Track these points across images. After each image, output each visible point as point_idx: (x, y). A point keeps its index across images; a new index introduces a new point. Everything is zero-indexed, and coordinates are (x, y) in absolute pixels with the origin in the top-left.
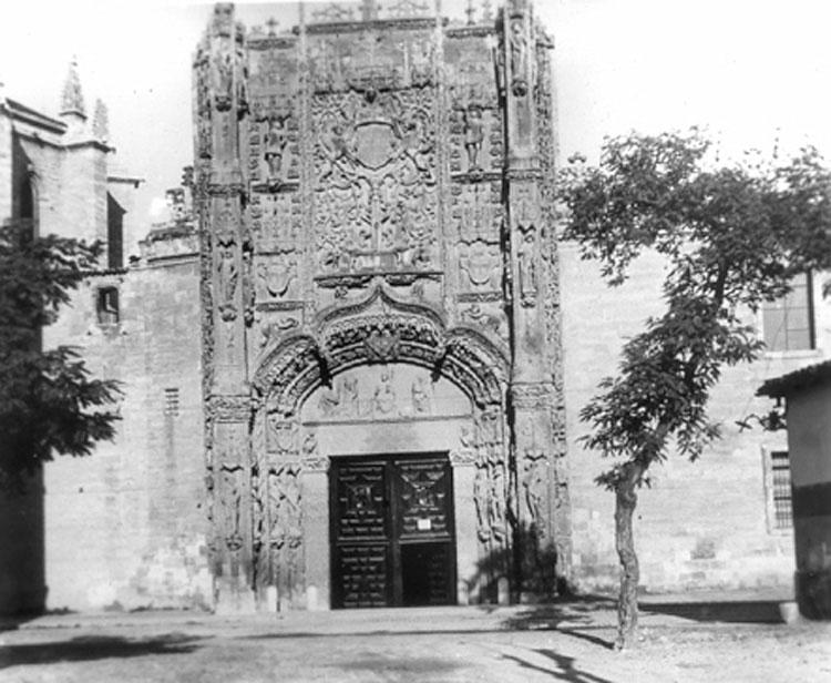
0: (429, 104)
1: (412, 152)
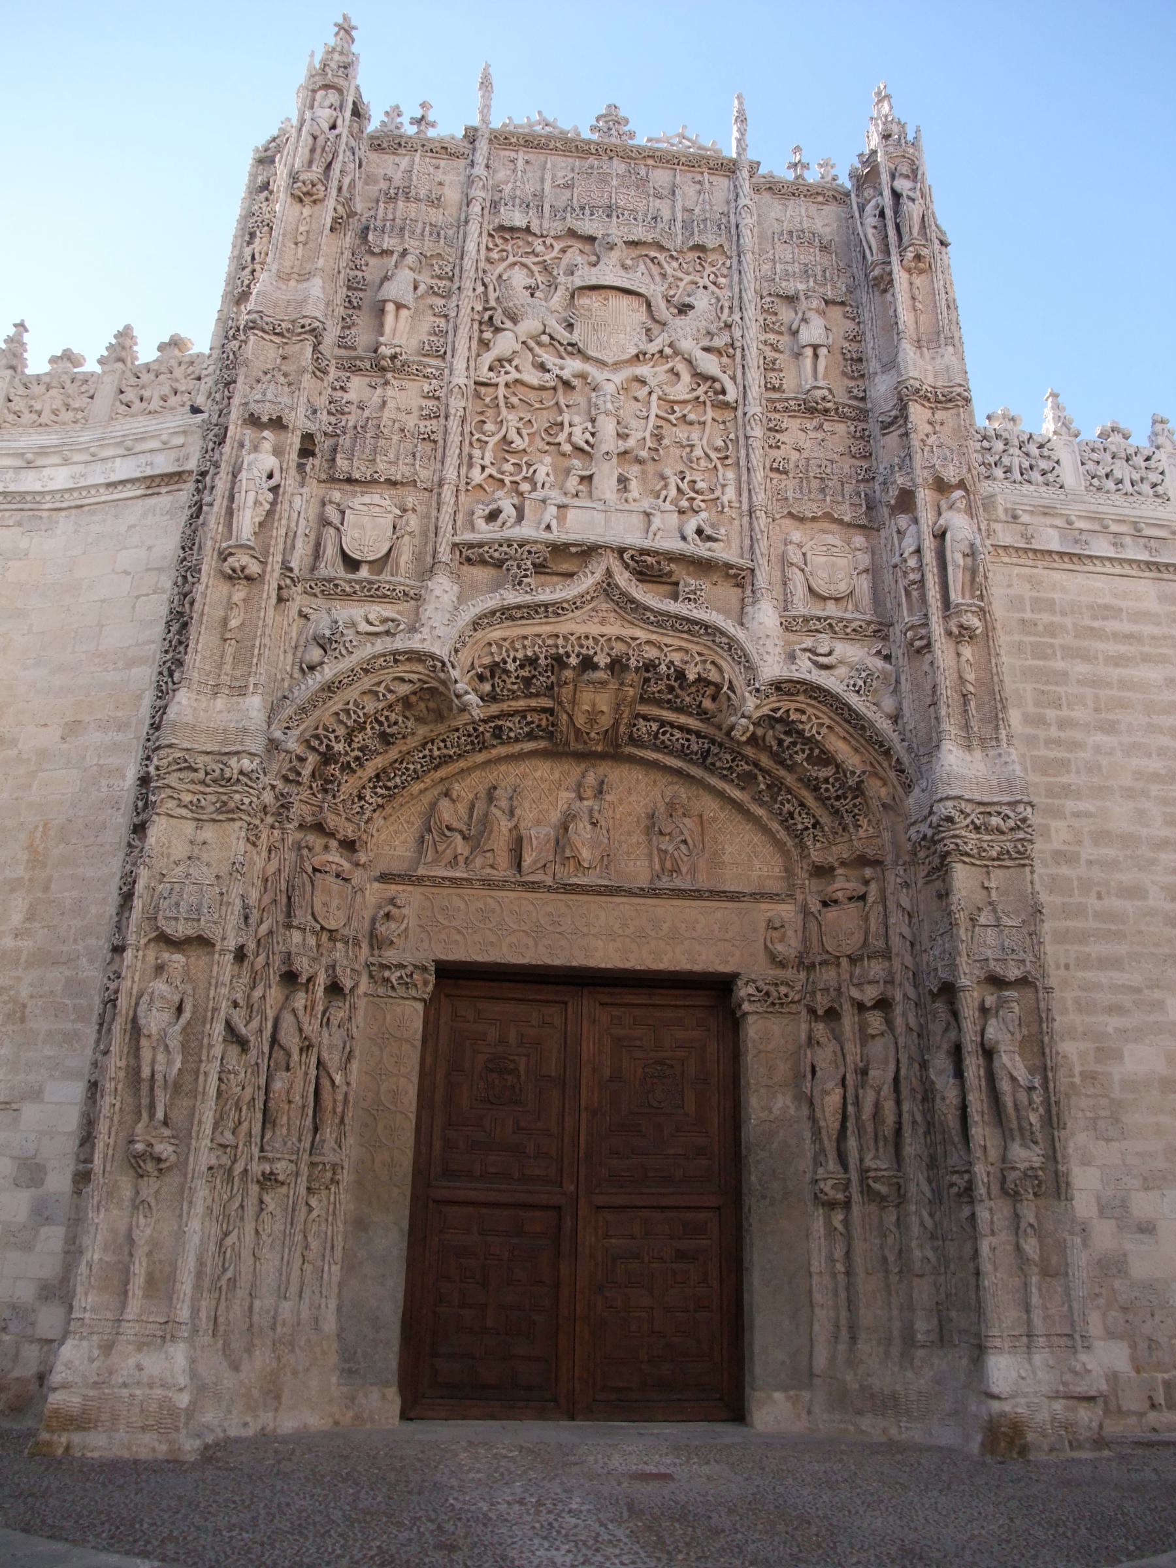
0: (722, 280)
1: (687, 345)
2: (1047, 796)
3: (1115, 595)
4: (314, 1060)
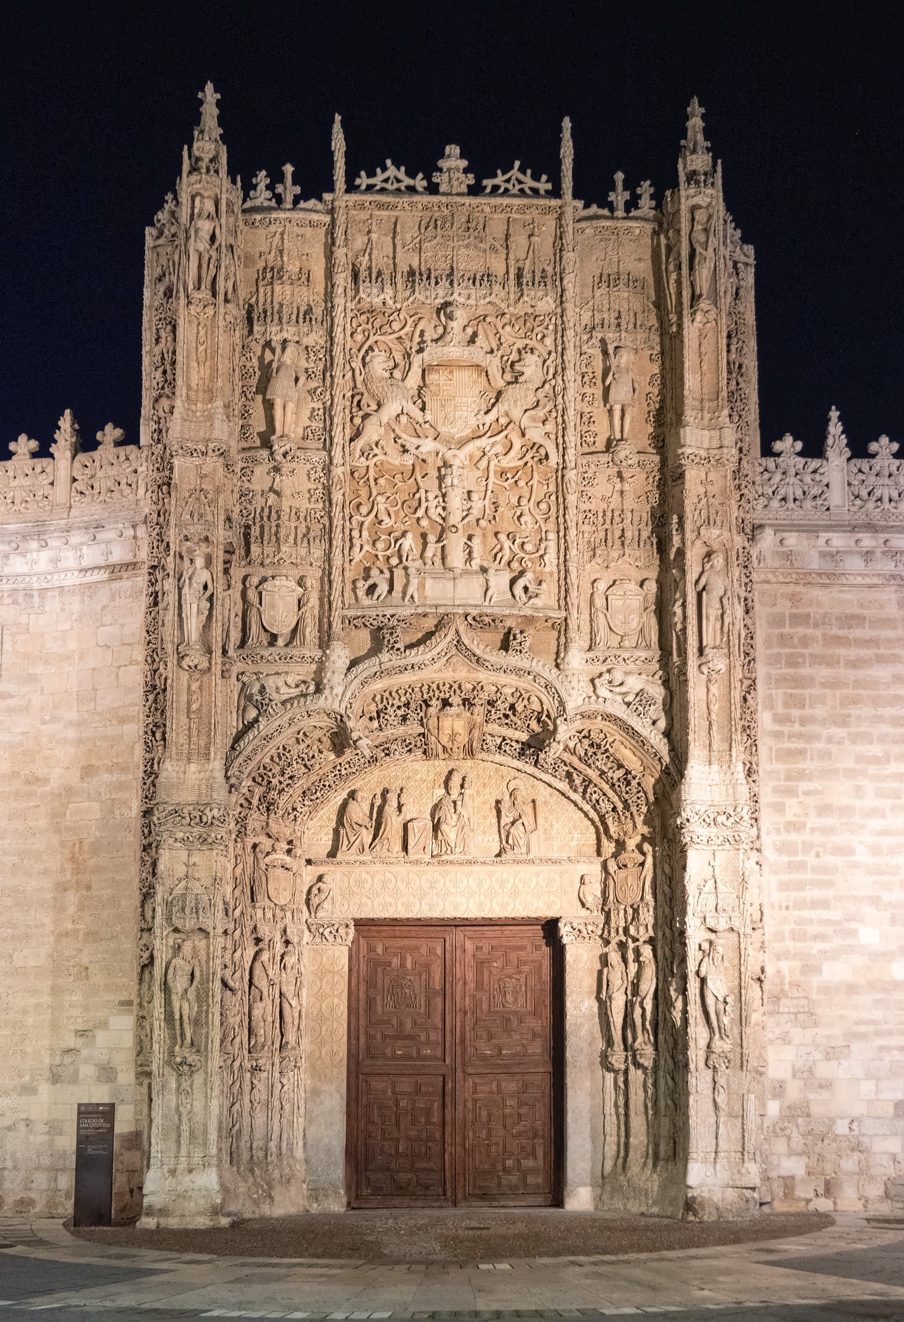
1: (516, 414)
2: (785, 780)
3: (862, 606)
4: (277, 992)
